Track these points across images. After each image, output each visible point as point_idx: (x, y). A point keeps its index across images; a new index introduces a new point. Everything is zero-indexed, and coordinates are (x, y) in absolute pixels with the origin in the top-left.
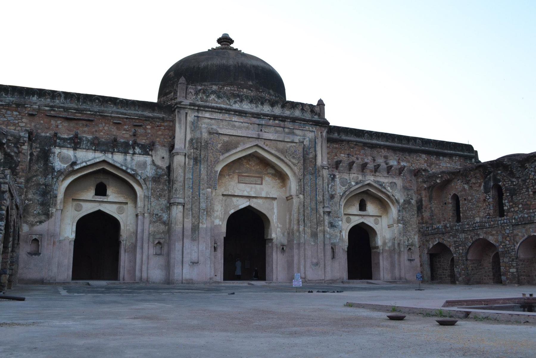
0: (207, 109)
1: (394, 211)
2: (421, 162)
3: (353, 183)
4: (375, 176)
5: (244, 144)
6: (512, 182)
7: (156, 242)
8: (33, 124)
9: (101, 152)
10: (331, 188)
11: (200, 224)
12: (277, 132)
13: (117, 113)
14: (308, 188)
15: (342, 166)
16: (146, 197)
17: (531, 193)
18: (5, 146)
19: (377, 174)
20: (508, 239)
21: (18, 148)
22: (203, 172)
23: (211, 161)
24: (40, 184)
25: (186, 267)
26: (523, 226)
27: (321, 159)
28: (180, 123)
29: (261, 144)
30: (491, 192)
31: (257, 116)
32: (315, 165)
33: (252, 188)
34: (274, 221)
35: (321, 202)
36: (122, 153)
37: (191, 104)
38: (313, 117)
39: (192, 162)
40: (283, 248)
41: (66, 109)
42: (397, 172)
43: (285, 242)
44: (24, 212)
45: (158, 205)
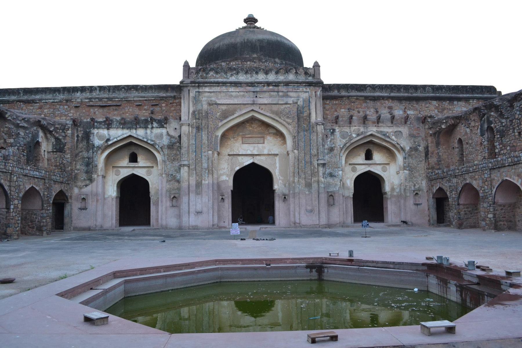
0: (206, 85)
1: (400, 157)
2: (432, 109)
3: (354, 135)
4: (378, 126)
5: (241, 110)
6: (502, 123)
7: (172, 196)
8: (78, 114)
9: (128, 129)
10: (331, 141)
11: (203, 181)
12: (271, 96)
13: (138, 97)
14: (302, 144)
15: (342, 121)
16: (164, 161)
17: (517, 134)
18: (53, 133)
19: (380, 124)
20: (486, 183)
21: (65, 132)
22: (205, 137)
23: (211, 128)
24: (85, 158)
25: (192, 216)
26: (498, 169)
27: (316, 116)
28: (184, 99)
29: (256, 108)
30: (486, 134)
31: (252, 84)
32: (310, 122)
33: (254, 147)
34: (277, 174)
35: (315, 155)
36: (143, 128)
37: (192, 82)
38: (307, 79)
39: (194, 130)
40: (285, 198)
41: (100, 99)
42: (403, 121)
43: (286, 192)
44: (73, 178)
45: (171, 167)
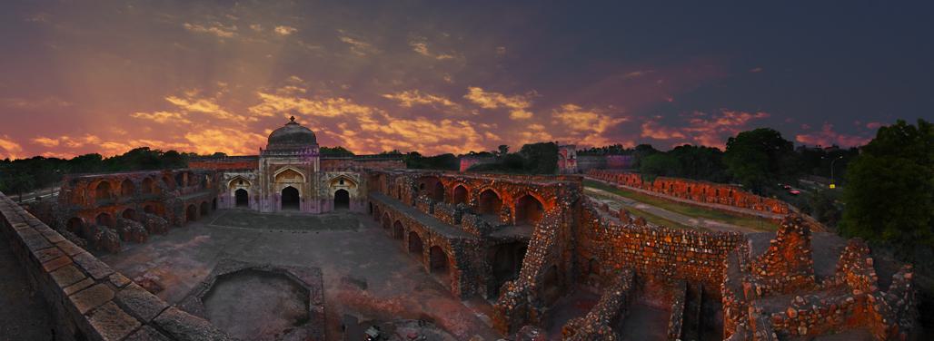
2: (370, 166)
